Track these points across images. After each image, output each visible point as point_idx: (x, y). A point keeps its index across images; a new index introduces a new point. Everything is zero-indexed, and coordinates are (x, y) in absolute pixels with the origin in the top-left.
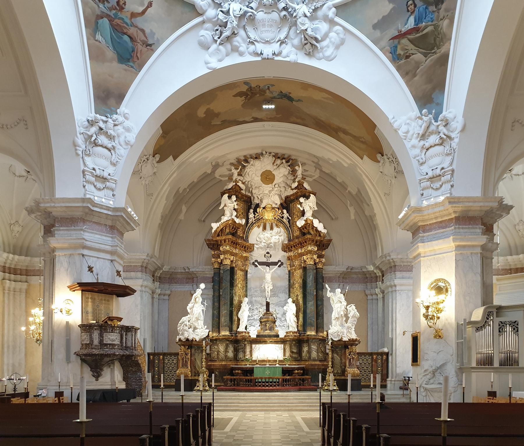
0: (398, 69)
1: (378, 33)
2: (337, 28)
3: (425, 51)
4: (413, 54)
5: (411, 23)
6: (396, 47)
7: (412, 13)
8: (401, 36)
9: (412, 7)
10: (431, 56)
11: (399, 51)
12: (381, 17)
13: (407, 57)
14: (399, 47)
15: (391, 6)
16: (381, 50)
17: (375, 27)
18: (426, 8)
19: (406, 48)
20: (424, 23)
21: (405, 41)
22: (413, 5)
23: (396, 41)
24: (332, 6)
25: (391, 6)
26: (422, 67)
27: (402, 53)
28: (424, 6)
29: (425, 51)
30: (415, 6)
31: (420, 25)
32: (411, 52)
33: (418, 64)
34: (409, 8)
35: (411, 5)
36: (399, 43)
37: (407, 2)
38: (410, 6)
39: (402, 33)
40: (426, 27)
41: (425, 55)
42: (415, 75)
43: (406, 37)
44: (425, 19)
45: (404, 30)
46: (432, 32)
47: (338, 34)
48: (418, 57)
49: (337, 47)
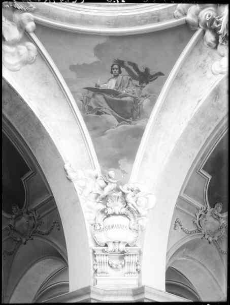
0: (86, 120)
1: (73, 75)
2: (30, 45)
3: (120, 117)
4: (106, 113)
5: (112, 85)
6: (90, 98)
7: (116, 76)
8: (97, 90)
9: (117, 71)
10: (125, 124)
11: (92, 103)
12: (81, 63)
13: (99, 113)
14: (92, 99)
15: (95, 59)
16: (73, 92)
17: (73, 68)
18: (130, 79)
19: (100, 104)
20: (124, 91)
21: (100, 97)
22: (118, 70)
23: (91, 93)
24: (33, 19)
25: (95, 59)
26: (113, 129)
27: (94, 107)
28: (129, 77)
29: (120, 117)
30: (120, 72)
31: (120, 90)
32: (104, 110)
33: (108, 125)
34: (113, 70)
35: (116, 69)
36: (94, 96)
37: (113, 65)
38: (115, 70)
39: (100, 88)
40: (125, 96)
41: (119, 120)
42: (103, 134)
43: (102, 94)
44: (127, 87)
45: (102, 87)
46: (130, 102)
47: (29, 50)
48: (111, 118)
49: (26, 63)
